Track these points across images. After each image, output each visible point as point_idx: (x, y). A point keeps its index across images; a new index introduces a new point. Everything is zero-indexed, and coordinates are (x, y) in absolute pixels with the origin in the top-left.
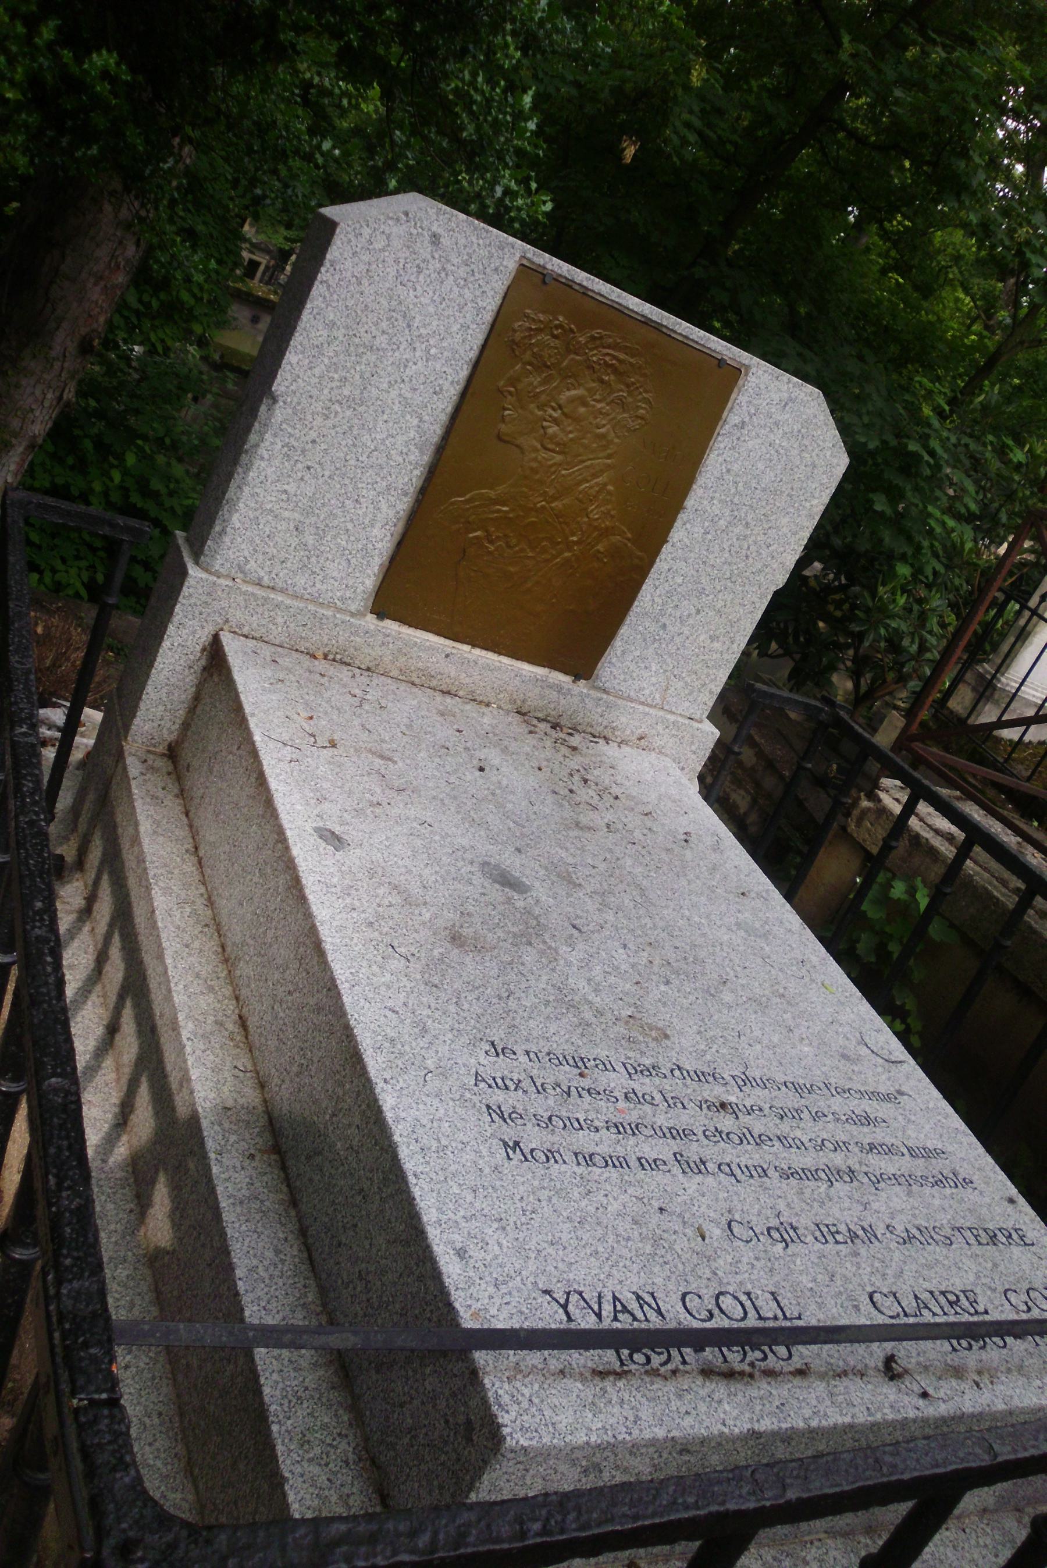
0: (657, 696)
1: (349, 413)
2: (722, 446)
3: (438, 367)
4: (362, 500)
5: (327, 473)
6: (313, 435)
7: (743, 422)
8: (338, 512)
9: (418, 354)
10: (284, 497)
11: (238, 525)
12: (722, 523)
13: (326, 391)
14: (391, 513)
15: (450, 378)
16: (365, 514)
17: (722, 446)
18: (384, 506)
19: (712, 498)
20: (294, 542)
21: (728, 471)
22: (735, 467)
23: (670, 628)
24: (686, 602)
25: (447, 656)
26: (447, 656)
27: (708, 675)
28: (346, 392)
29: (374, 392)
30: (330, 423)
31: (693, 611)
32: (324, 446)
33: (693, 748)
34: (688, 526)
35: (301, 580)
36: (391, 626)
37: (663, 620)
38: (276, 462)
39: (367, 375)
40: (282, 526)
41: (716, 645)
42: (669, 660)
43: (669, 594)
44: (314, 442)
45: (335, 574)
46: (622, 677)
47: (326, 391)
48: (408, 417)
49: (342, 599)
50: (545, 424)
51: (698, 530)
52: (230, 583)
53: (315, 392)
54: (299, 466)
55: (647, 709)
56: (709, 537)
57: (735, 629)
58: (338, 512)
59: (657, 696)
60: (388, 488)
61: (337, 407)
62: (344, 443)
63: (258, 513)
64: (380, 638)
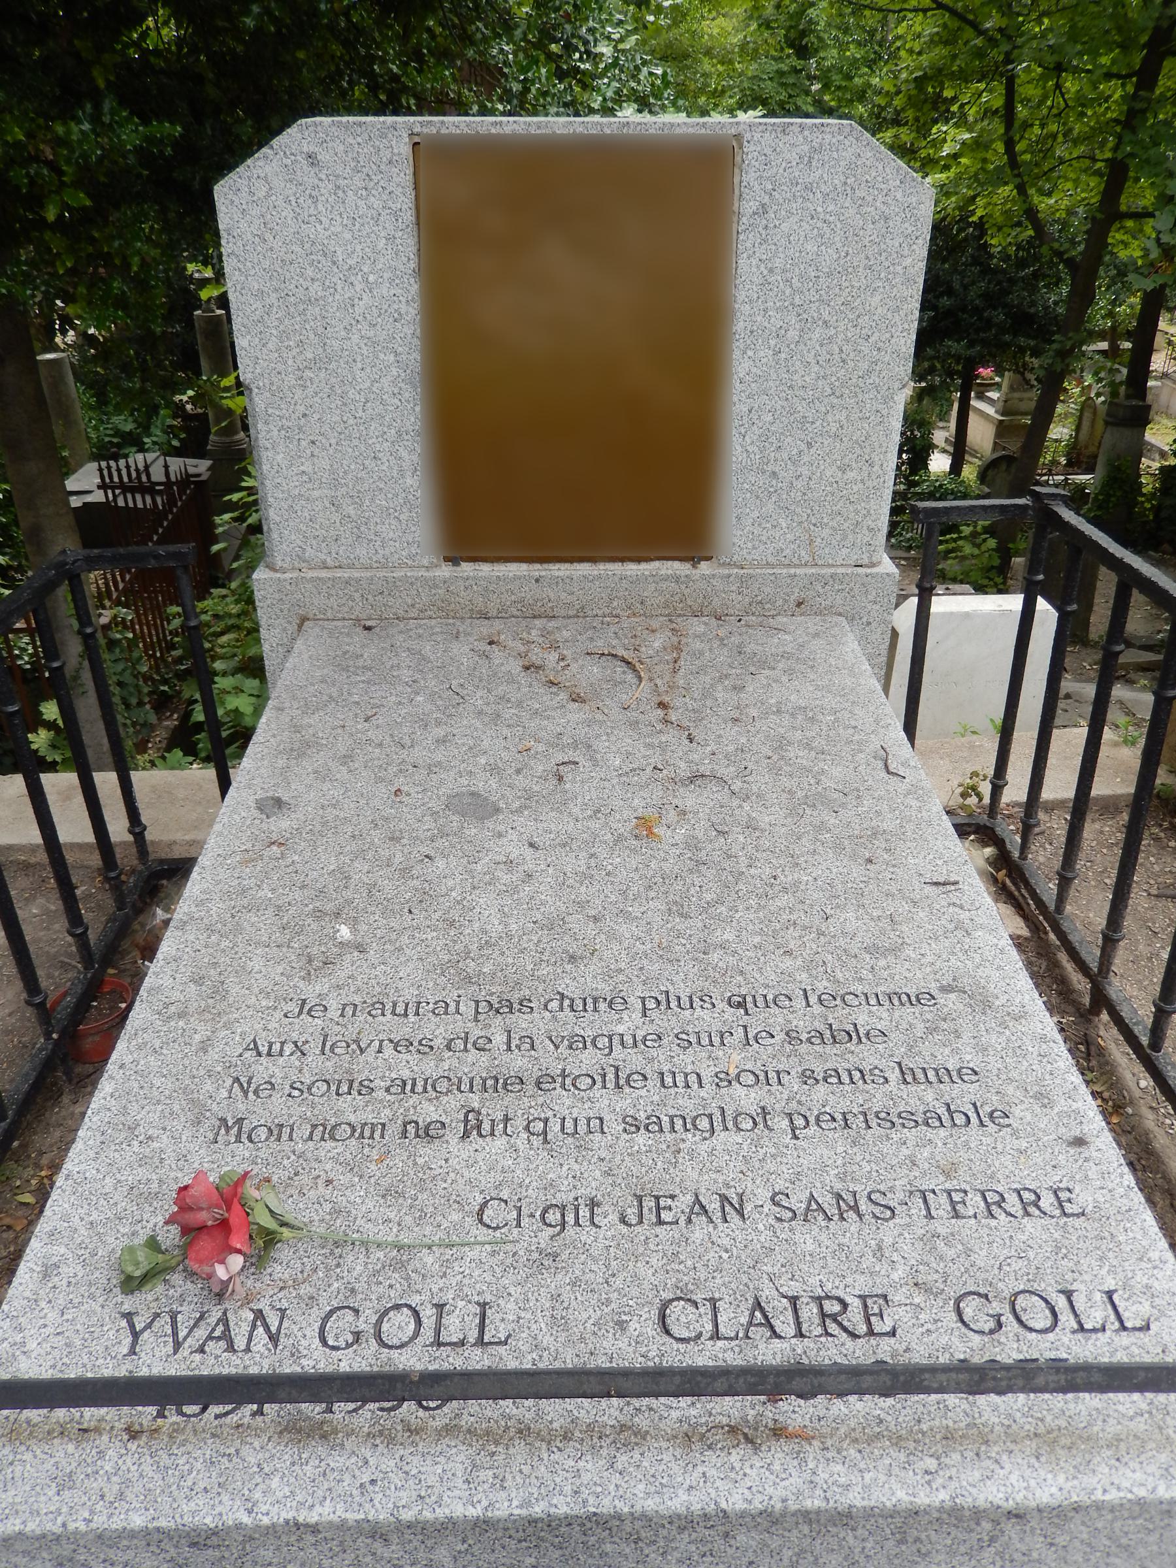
1: (322, 375)
2: (748, 245)
3: (385, 292)
4: (380, 455)
5: (333, 441)
6: (301, 409)
7: (763, 206)
8: (363, 474)
9: (358, 287)
10: (305, 478)
11: (278, 519)
12: (793, 334)
13: (290, 362)
14: (415, 458)
15: (403, 300)
16: (390, 467)
17: (748, 245)
18: (405, 454)
20: (336, 517)
21: (771, 271)
22: (778, 263)
23: (782, 474)
24: (789, 439)
27: (857, 512)
28: (310, 356)
29: (336, 344)
30: (310, 391)
31: (803, 446)
32: (316, 416)
34: (750, 353)
35: (361, 551)
37: (770, 468)
38: (281, 448)
39: (320, 330)
40: (318, 506)
41: (851, 475)
42: (798, 510)
43: (765, 438)
44: (305, 415)
45: (391, 535)
46: (750, 545)
47: (290, 362)
48: (382, 356)
49: (410, 557)
52: (295, 574)
53: (280, 367)
54: (303, 443)
56: (783, 356)
57: (867, 450)
58: (363, 474)
60: (399, 434)
61: (309, 374)
62: (333, 406)
63: (290, 502)
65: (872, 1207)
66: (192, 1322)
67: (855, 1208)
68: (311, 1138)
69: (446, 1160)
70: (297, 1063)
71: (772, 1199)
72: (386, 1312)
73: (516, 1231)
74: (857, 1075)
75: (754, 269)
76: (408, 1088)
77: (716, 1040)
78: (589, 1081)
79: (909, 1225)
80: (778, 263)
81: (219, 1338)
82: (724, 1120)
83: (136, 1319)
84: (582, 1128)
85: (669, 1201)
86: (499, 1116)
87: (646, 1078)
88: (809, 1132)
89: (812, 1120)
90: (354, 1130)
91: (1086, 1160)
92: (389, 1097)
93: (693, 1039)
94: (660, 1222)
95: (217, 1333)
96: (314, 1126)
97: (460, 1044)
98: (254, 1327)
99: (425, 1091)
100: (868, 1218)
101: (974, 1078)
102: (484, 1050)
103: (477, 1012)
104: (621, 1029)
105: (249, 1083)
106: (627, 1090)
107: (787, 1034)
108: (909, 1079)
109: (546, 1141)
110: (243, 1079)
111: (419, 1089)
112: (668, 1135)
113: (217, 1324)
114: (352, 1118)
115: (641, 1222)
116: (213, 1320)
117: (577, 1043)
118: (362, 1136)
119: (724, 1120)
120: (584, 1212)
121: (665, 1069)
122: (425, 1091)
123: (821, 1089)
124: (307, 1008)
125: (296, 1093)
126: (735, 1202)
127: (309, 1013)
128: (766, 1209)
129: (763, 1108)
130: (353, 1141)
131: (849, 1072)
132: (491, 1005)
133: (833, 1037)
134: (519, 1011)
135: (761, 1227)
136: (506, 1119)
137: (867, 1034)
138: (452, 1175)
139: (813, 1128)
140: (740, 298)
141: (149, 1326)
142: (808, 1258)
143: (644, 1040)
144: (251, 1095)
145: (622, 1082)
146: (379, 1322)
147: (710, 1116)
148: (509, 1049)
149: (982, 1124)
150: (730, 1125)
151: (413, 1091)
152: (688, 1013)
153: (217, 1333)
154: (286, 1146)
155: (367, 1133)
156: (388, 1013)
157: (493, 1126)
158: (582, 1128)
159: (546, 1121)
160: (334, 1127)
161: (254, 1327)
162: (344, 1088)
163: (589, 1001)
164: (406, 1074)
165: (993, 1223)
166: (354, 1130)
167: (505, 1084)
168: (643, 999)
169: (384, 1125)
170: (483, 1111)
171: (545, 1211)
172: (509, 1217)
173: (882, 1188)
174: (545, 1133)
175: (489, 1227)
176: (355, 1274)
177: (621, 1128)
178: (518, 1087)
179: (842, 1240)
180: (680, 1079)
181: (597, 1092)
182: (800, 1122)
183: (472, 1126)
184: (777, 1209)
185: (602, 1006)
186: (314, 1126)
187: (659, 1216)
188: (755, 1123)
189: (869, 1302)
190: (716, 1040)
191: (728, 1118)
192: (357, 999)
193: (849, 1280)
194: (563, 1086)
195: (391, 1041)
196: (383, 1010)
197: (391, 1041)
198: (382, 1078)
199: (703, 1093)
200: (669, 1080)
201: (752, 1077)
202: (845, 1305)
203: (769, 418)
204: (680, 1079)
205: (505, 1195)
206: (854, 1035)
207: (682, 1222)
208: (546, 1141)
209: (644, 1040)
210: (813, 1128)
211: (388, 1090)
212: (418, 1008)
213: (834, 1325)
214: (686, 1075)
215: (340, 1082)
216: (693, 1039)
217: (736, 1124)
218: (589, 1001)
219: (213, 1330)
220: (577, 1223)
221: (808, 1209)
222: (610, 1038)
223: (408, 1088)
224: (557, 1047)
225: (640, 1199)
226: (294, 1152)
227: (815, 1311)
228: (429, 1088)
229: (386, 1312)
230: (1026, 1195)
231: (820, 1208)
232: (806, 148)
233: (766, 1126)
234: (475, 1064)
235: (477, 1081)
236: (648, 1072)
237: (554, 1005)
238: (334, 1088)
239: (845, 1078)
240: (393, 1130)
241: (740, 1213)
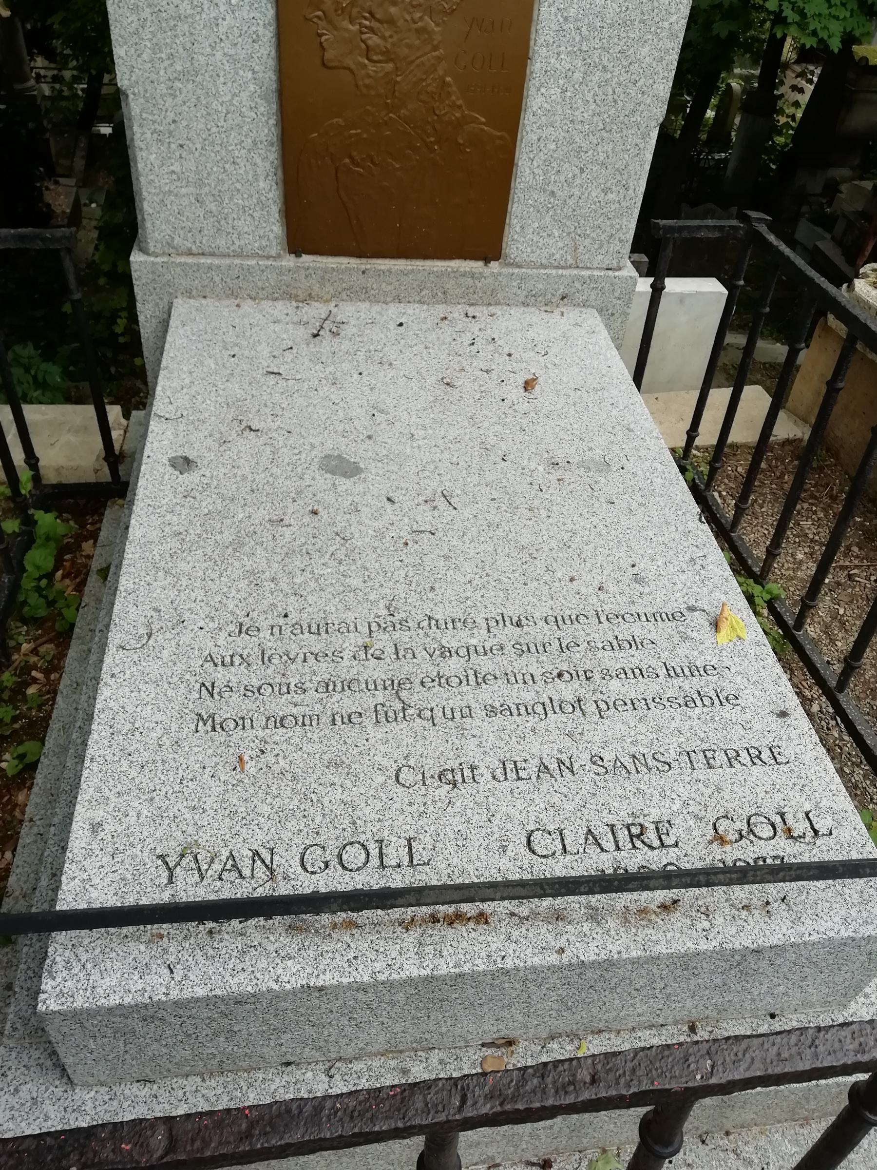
0: (569, 257)
1: (190, 86)
3: (245, 14)
4: (238, 161)
5: (199, 146)
6: (171, 115)
8: (224, 176)
9: (222, 8)
13: (162, 73)
14: (268, 165)
15: (261, 23)
16: (246, 172)
18: (258, 161)
23: (559, 193)
24: (567, 165)
25: (364, 272)
26: (364, 272)
27: (612, 226)
28: (179, 68)
29: (202, 59)
30: (179, 100)
31: (577, 171)
32: (184, 123)
33: (616, 294)
36: (307, 259)
37: (550, 188)
38: (154, 149)
39: (189, 45)
41: (611, 196)
43: (548, 163)
44: (174, 121)
47: (162, 73)
48: (241, 72)
50: (364, 37)
51: (555, 91)
53: (154, 76)
54: (173, 146)
55: (560, 272)
57: (625, 177)
58: (224, 176)
59: (569, 257)
60: (255, 143)
61: (178, 84)
62: (199, 115)
64: (303, 272)
75: (553, 17)
77: (541, 649)
79: (680, 774)
80: (572, 12)
84: (457, 715)
91: (789, 726)
92: (318, 695)
96: (268, 719)
101: (715, 672)
103: (370, 631)
104: (474, 641)
105: (213, 687)
106: (483, 686)
108: (672, 673)
110: (207, 684)
111: (339, 688)
118: (304, 724)
120: (467, 773)
125: (250, 694)
128: (587, 768)
130: (298, 728)
132: (379, 626)
140: (540, 41)
144: (215, 695)
149: (721, 704)
150: (557, 709)
151: (334, 690)
154: (250, 733)
158: (457, 715)
165: (733, 770)
170: (387, 704)
175: (404, 786)
181: (464, 688)
182: (603, 706)
185: (459, 625)
186: (268, 719)
190: (541, 649)
203: (553, 146)
204: (520, 677)
216: (525, 648)
222: (468, 648)
223: (331, 687)
224: (431, 656)
228: (346, 688)
230: (752, 751)
237: (425, 624)
238: (276, 689)
239: (630, 673)
240: (326, 719)
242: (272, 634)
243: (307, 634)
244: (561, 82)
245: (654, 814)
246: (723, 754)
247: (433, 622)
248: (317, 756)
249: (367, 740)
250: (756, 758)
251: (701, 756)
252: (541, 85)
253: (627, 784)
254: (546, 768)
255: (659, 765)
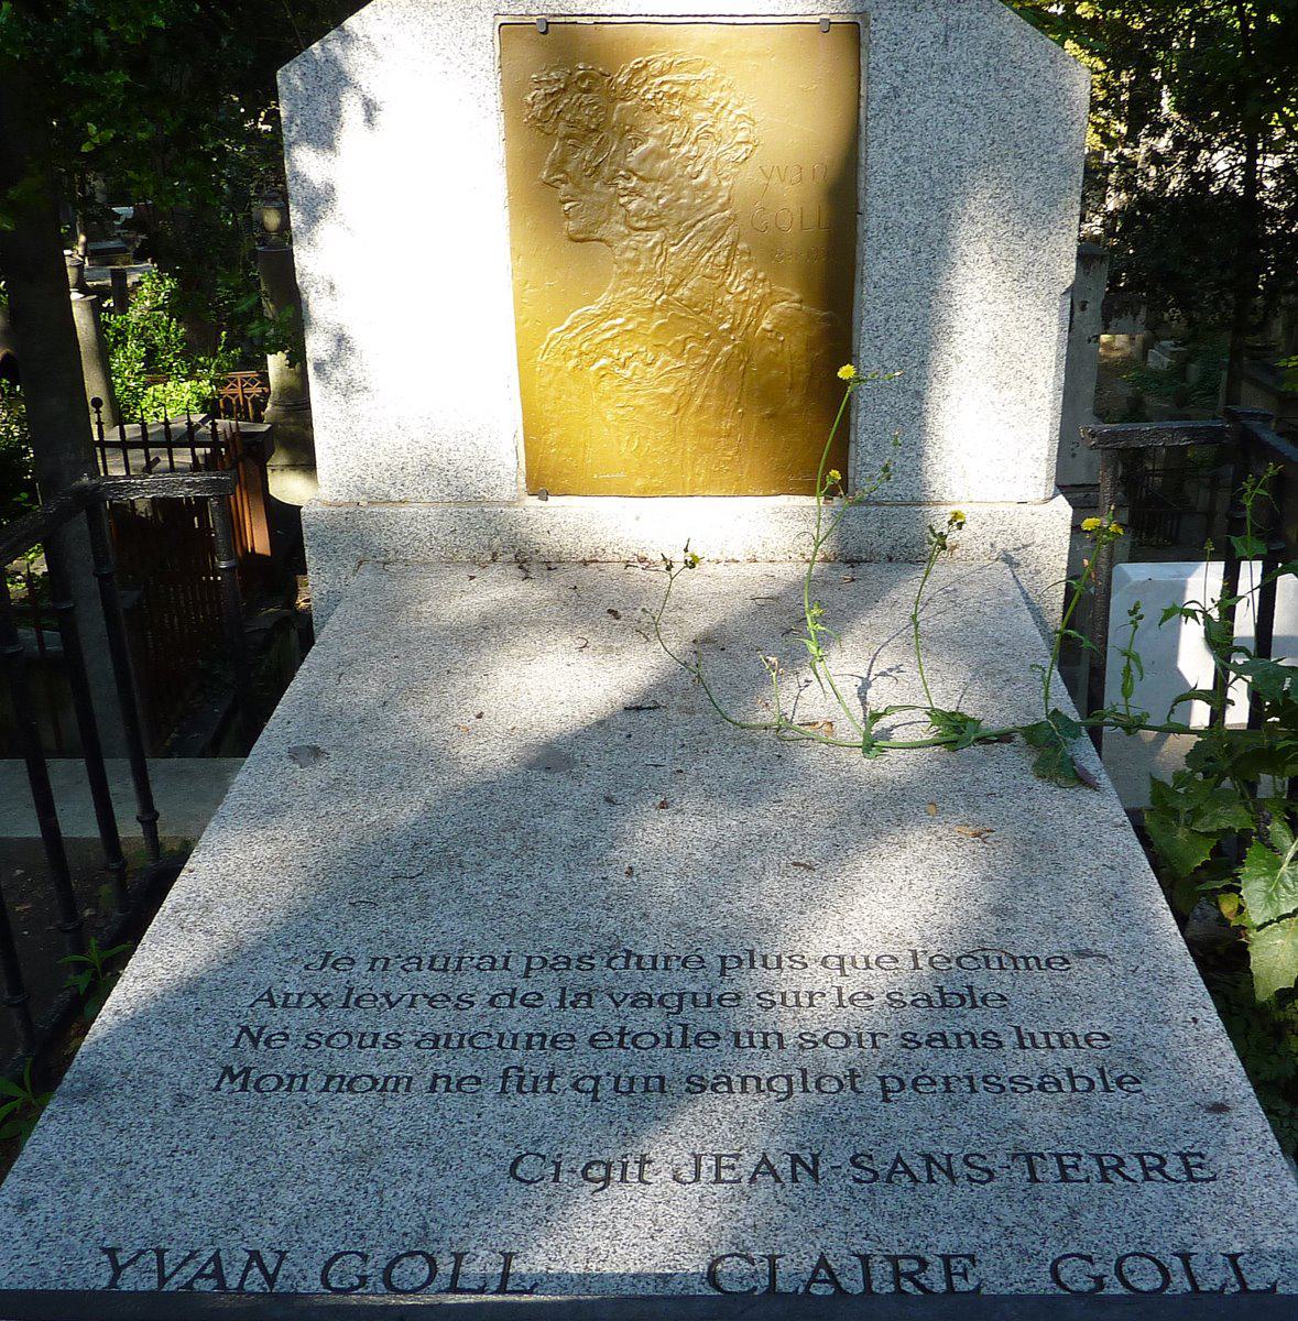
2: (879, 132)
7: (895, 88)
17: (879, 132)
19: (902, 205)
21: (906, 160)
34: (885, 253)
56: (924, 255)
65: (967, 1169)
66: (180, 1260)
67: (949, 1173)
68: (326, 1089)
69: (479, 1115)
70: (317, 1015)
71: (853, 1160)
72: (399, 1258)
73: (552, 1186)
74: (966, 1039)
76: (442, 1042)
77: (805, 1001)
78: (652, 1039)
81: (208, 1277)
82: (804, 1082)
83: (118, 1255)
84: (638, 1089)
85: (732, 1161)
86: (545, 1072)
87: (718, 1037)
88: (904, 1095)
89: (909, 1083)
90: (375, 1082)
92: (419, 1051)
93: (777, 998)
94: (718, 1180)
95: (208, 1271)
96: (330, 1078)
97: (506, 1000)
98: (249, 1267)
99: (461, 1045)
100: (962, 1181)
101: (1104, 1044)
102: (533, 1006)
103: (528, 968)
104: (693, 988)
106: (695, 1049)
107: (888, 996)
108: (1028, 1043)
109: (595, 1099)
111: (454, 1043)
112: (738, 1096)
113: (209, 1263)
114: (375, 1071)
115: (697, 1179)
116: (204, 1259)
117: (641, 1000)
118: (384, 1089)
119: (804, 1082)
121: (742, 1028)
122: (461, 1045)
123: (924, 1053)
124: (331, 961)
126: (809, 1162)
127: (334, 965)
129: (852, 1071)
130: (374, 1094)
131: (958, 1036)
133: (943, 1000)
134: (578, 967)
135: (836, 1187)
136: (552, 1077)
137: (984, 1000)
138: (485, 1130)
139: (909, 1091)
141: (133, 1261)
142: (887, 1218)
143: (720, 999)
145: (690, 1041)
146: (391, 1266)
147: (789, 1078)
148: (562, 1005)
149: (1107, 1089)
150: (811, 1086)
151: (446, 1046)
152: (773, 972)
153: (208, 1271)
154: (298, 1097)
155: (390, 1086)
156: (425, 967)
157: (535, 1082)
158: (638, 1089)
159: (597, 1079)
160: (353, 1080)
161: (249, 1267)
162: (368, 1041)
163: (661, 959)
164: (440, 1029)
166: (375, 1082)
167: (554, 1041)
168: (723, 958)
169: (410, 1079)
170: (526, 1068)
171: (588, 1166)
172: (546, 1172)
173: (983, 1151)
174: (595, 1091)
176: (366, 1221)
177: (684, 1088)
178: (569, 1044)
179: (928, 1201)
180: (758, 1039)
181: (659, 1051)
182: (893, 1084)
183: (515, 1081)
184: (858, 1171)
185: (675, 964)
186: (330, 1078)
187: (718, 1174)
188: (841, 1085)
189: (953, 1262)
190: (805, 1001)
191: (809, 1079)
192: (390, 954)
193: (933, 1240)
194: (621, 1044)
195: (425, 996)
196: (419, 964)
197: (425, 996)
198: (413, 1032)
199: (784, 1054)
200: (745, 1041)
201: (841, 1039)
202: (923, 1264)
203: (910, 328)
204: (758, 1039)
205: (543, 1150)
206: (968, 999)
207: (746, 1179)
208: (595, 1099)
209: (720, 999)
210: (909, 1091)
211: (418, 1044)
212: (460, 962)
213: (909, 1284)
214: (766, 1035)
215: (363, 1035)
216: (777, 998)
217: (818, 1086)
218: (661, 959)
219: (204, 1268)
220: (623, 1179)
221: (893, 1171)
222: (681, 996)
223: (442, 1042)
224: (617, 1005)
225: (698, 1158)
226: (306, 1102)
227: (889, 1269)
228: (466, 1043)
229: (399, 1258)
231: (907, 1171)
232: (941, 26)
233: (853, 1088)
234: (517, 1020)
235: (523, 1038)
236: (722, 1031)
238: (356, 1041)
239: (952, 1041)
240: (422, 1084)
241: (814, 1173)
242: (371, 969)
243: (426, 970)
244: (911, 241)
245: (945, 1242)
246: (1093, 1162)
247: (633, 960)
248: (393, 1132)
249: (479, 1115)
250: (1154, 1168)
251: (1052, 1163)
252: (882, 247)
253: (907, 1198)
254: (771, 1167)
255: (974, 1173)
